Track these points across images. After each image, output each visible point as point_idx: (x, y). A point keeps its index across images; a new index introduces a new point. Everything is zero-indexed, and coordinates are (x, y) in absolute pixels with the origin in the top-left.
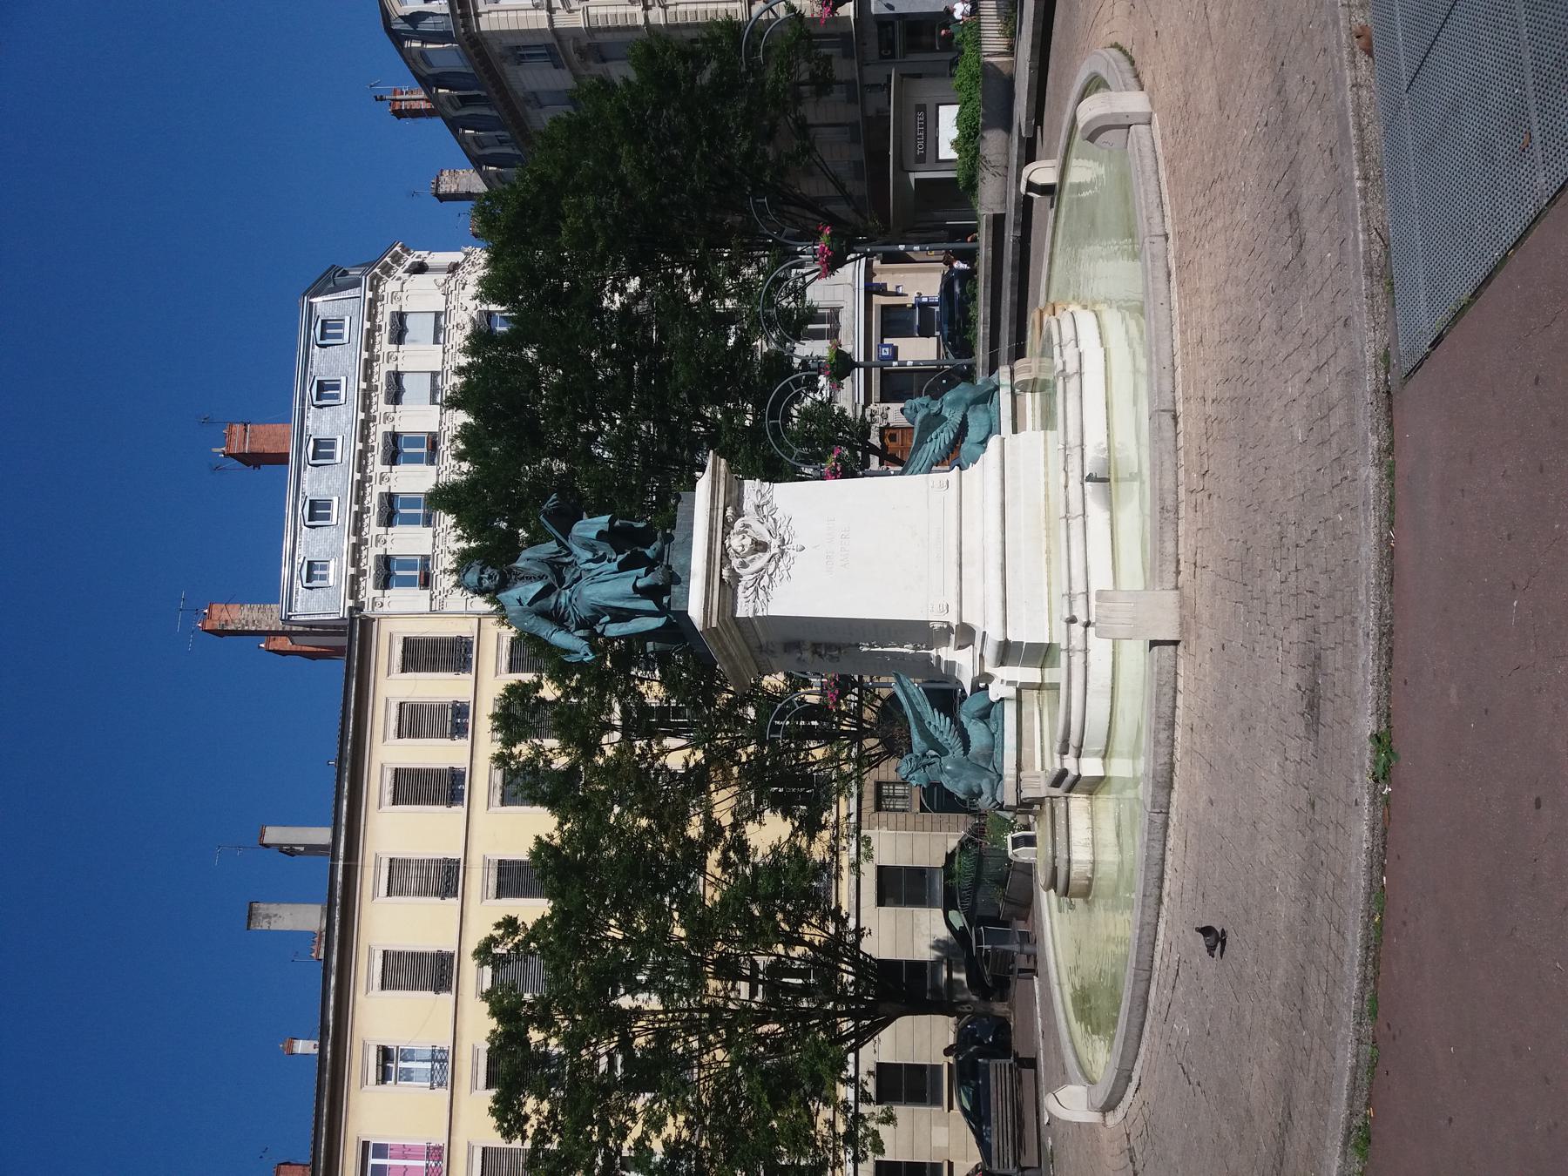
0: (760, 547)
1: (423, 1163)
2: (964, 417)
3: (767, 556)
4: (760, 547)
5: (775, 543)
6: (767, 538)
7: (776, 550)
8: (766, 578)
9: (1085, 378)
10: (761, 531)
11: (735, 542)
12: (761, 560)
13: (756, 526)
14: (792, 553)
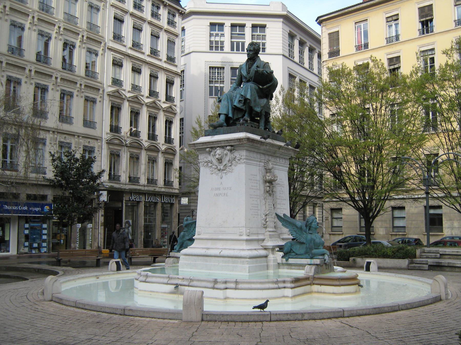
0: (220, 160)
1: (363, 43)
2: (302, 243)
3: (217, 164)
4: (220, 160)
5: (222, 167)
6: (224, 164)
7: (219, 168)
8: (211, 165)
9: (211, 290)
10: (225, 161)
11: (219, 151)
12: (215, 162)
13: (227, 159)
14: (220, 174)
